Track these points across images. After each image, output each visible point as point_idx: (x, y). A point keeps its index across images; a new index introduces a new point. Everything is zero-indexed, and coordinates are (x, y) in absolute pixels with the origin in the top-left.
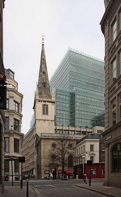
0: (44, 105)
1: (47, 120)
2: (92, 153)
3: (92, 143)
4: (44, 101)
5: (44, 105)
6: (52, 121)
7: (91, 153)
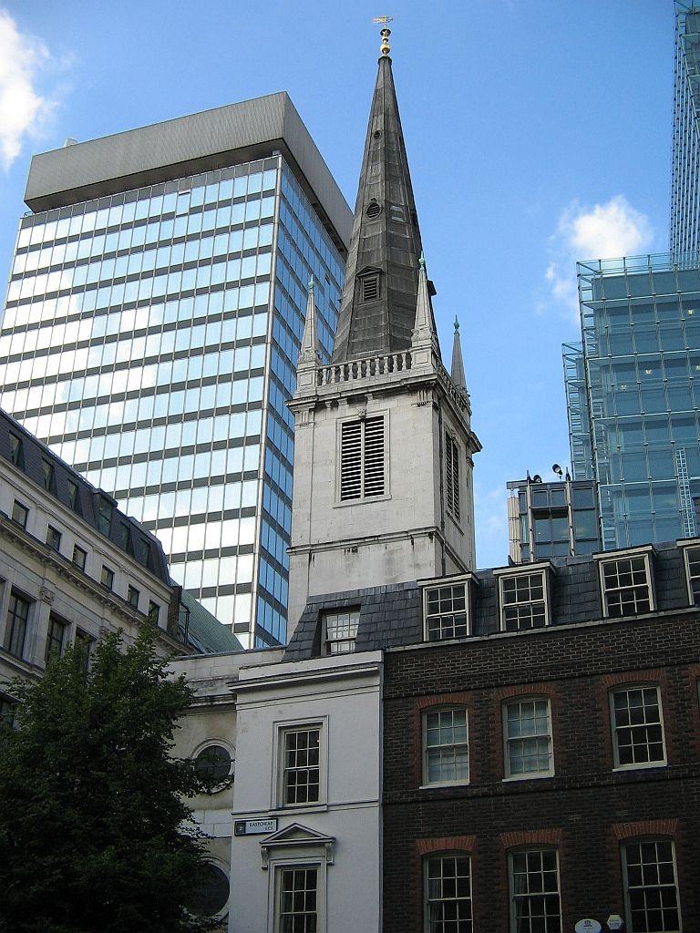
0: (349, 428)
1: (376, 539)
2: (296, 830)
3: (298, 709)
4: (356, 399)
5: (349, 428)
6: (410, 536)
7: (285, 824)
